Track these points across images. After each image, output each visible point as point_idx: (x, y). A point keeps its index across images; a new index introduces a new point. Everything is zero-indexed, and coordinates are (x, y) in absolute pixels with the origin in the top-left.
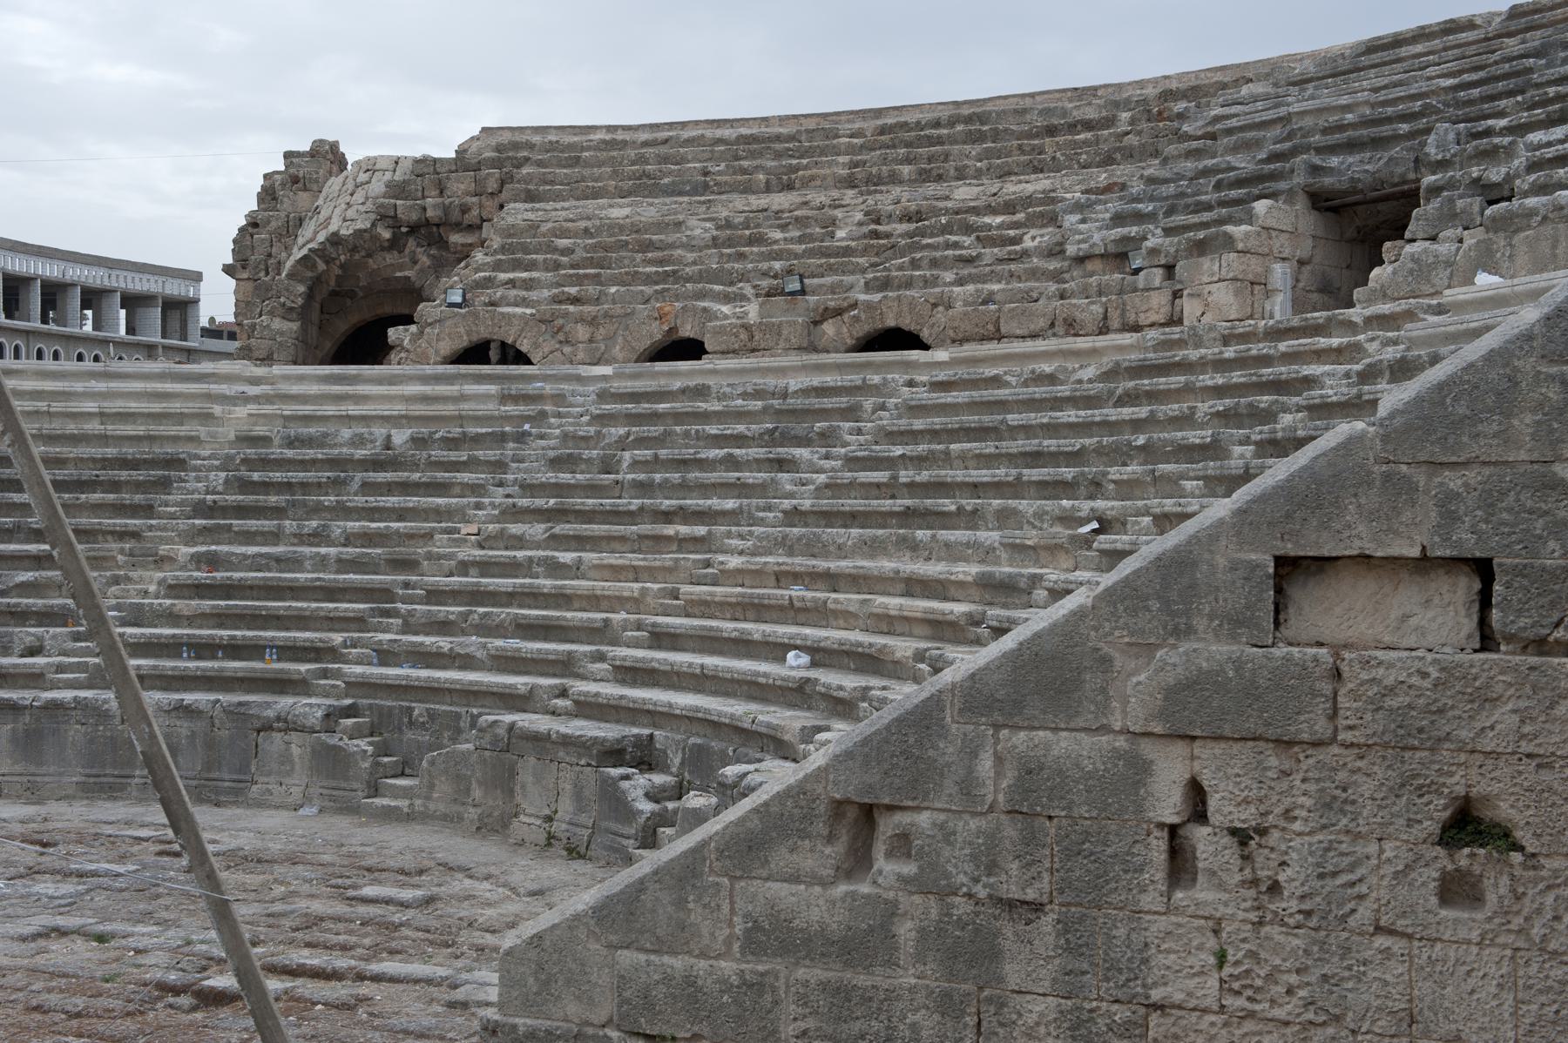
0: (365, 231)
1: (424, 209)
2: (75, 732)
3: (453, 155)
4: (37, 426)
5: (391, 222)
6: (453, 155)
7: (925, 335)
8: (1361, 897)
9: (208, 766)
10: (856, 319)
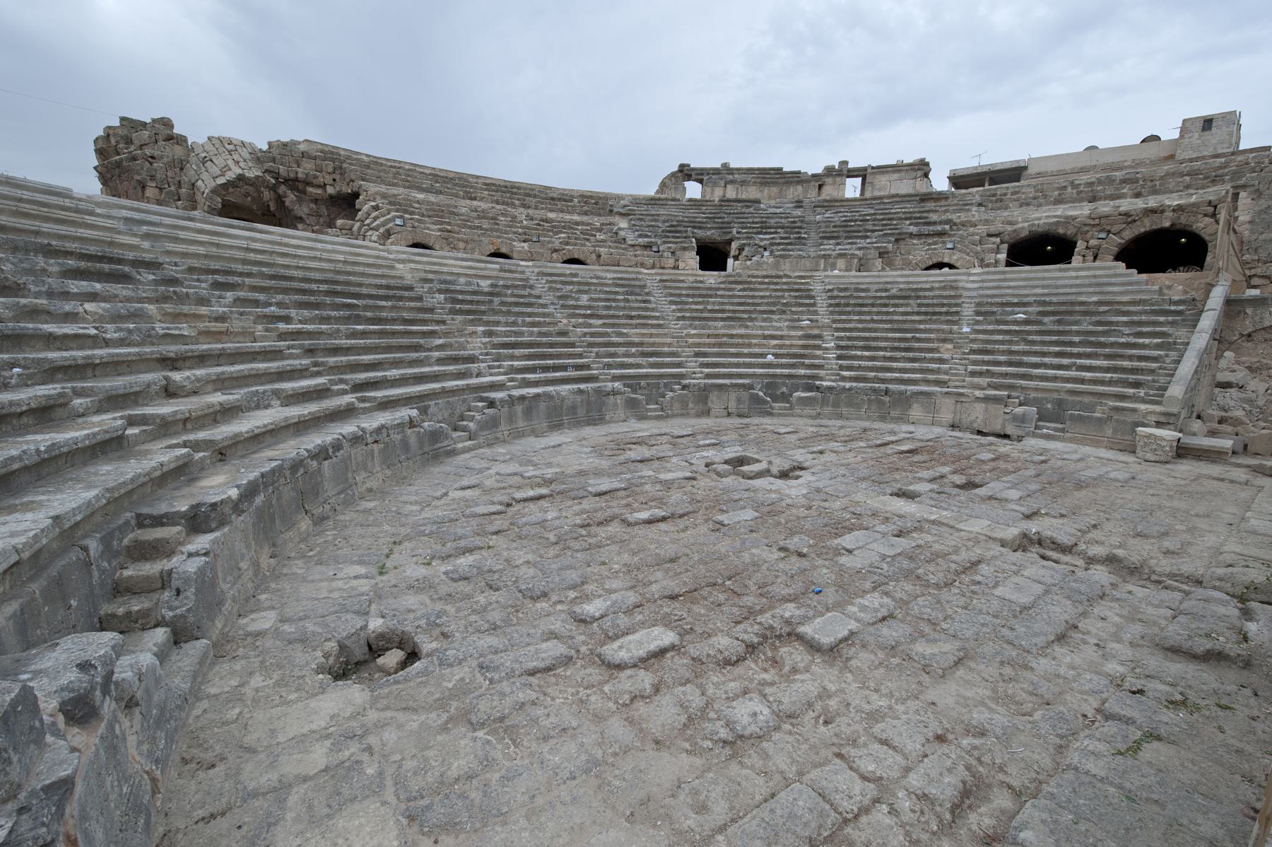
2: (543, 406)
3: (265, 147)
6: (265, 147)
7: (588, 261)
9: (587, 412)
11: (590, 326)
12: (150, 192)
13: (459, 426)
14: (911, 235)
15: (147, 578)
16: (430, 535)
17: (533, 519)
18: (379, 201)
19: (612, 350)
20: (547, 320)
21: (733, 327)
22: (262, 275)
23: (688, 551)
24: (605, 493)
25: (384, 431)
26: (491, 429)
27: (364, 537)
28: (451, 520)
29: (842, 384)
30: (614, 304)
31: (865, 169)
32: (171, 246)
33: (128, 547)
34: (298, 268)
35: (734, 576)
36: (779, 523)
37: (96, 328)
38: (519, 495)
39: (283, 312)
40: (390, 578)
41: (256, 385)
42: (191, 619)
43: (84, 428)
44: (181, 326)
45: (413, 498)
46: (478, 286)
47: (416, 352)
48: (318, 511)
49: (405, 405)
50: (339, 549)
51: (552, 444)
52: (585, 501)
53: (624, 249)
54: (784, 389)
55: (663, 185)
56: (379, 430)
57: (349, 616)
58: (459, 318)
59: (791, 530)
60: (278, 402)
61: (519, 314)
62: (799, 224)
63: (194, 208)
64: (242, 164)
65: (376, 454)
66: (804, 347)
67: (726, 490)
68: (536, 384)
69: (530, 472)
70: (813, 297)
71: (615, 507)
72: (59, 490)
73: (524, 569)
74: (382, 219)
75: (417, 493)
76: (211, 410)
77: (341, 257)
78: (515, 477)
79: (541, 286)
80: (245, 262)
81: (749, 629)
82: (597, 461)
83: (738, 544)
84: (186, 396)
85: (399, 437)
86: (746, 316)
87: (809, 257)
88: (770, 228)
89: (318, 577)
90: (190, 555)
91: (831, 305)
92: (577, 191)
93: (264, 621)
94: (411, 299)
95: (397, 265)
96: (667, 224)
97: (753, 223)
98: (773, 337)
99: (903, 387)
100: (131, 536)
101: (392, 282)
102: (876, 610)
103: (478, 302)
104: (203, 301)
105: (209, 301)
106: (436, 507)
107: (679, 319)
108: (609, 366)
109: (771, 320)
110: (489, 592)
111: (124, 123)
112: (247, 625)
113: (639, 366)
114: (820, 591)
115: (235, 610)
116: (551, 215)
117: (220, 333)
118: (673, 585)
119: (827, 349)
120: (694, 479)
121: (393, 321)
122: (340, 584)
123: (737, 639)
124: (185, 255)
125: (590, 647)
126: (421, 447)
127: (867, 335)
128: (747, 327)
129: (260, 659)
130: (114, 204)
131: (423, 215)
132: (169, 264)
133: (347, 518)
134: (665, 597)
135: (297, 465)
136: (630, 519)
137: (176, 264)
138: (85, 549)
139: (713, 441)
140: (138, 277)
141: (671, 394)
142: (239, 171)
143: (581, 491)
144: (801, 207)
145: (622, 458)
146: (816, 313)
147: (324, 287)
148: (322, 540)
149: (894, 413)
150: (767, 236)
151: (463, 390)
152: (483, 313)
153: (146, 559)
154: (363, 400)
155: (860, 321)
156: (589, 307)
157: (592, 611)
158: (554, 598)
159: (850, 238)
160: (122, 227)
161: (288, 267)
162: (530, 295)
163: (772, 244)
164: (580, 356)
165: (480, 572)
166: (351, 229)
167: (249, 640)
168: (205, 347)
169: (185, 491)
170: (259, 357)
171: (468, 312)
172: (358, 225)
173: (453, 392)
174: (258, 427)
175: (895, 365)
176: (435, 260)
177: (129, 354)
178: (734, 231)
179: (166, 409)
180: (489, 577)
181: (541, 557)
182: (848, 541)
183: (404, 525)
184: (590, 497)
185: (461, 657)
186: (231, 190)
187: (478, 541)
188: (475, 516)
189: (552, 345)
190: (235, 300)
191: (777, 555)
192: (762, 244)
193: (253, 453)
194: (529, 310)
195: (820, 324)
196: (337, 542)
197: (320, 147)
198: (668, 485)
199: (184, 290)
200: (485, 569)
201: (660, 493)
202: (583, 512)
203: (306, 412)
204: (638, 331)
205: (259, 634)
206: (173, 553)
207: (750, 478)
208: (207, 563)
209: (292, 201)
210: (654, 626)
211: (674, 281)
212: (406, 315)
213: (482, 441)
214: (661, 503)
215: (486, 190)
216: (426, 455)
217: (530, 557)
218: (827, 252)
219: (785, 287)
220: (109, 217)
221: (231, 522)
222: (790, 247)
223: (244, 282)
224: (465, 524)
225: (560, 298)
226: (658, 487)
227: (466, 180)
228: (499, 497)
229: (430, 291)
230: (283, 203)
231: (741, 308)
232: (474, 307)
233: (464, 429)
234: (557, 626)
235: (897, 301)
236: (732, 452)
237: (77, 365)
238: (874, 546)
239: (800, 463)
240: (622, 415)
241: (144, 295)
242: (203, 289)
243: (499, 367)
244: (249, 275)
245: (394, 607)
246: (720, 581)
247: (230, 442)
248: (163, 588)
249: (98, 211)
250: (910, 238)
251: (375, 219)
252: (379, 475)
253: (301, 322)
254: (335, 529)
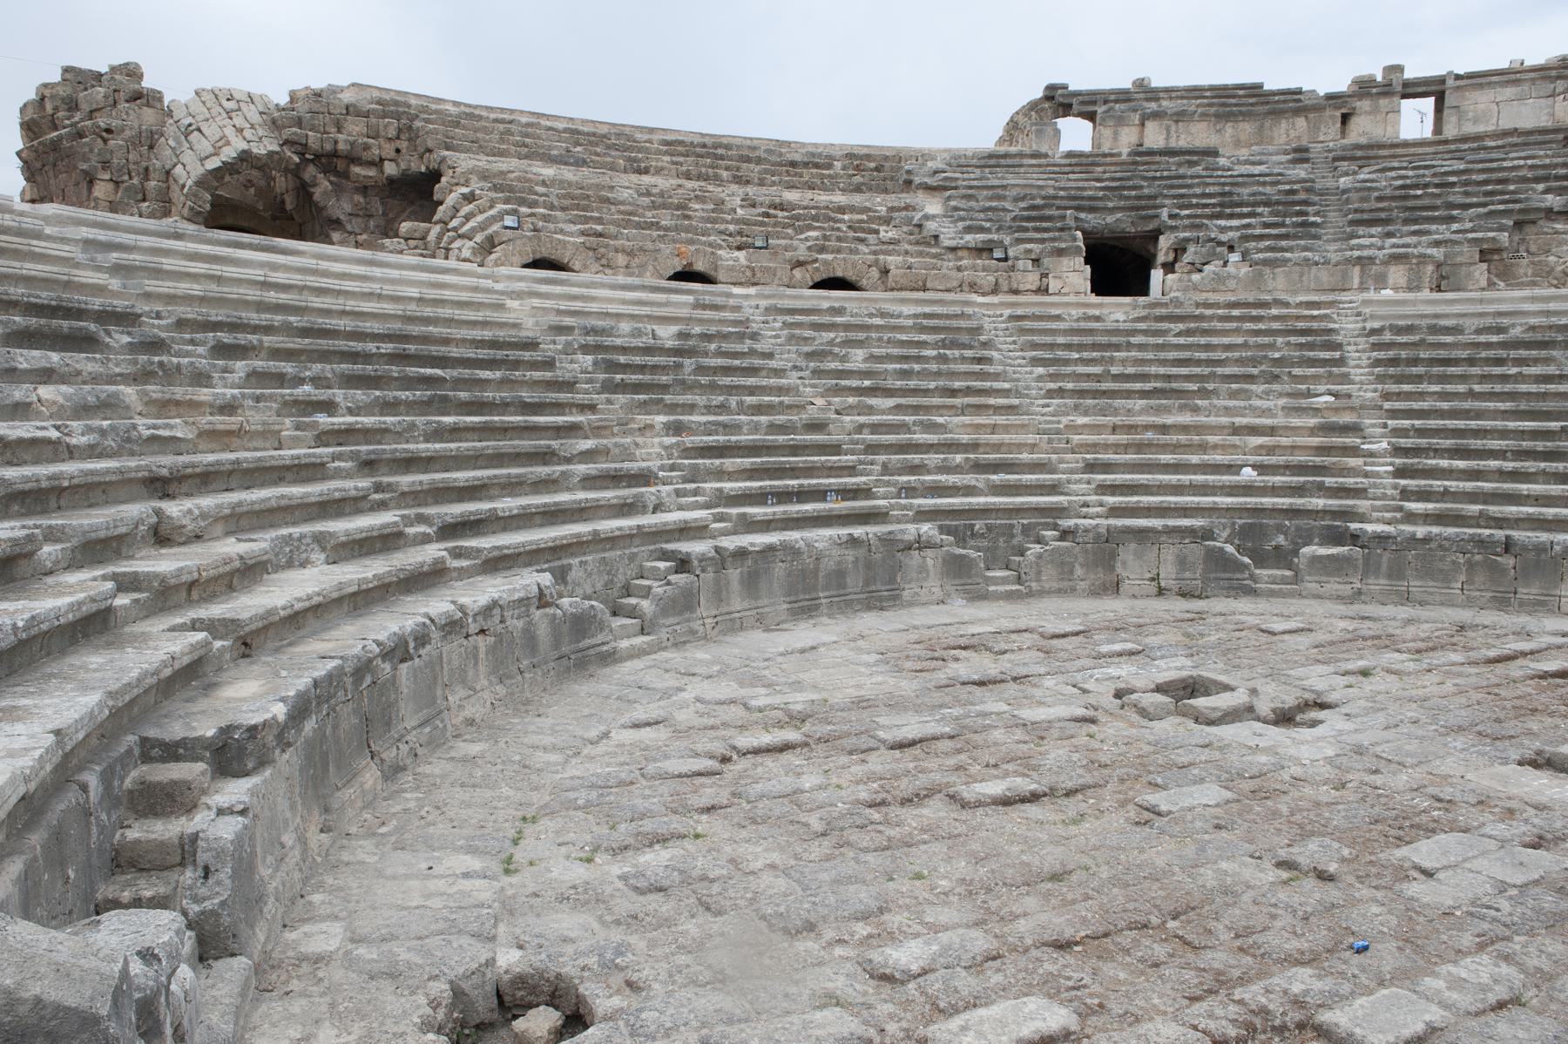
0: (277, 153)
1: (336, 142)
2: (779, 569)
4: (402, 307)
5: (299, 148)
6: (284, 100)
7: (864, 282)
9: (867, 583)
10: (817, 269)
11: (870, 410)
12: (101, 190)
13: (622, 607)
14: (1550, 213)
15: (162, 846)
16: (586, 807)
17: (775, 786)
18: (476, 185)
19: (915, 458)
20: (786, 400)
21: (1167, 410)
22: (288, 329)
23: (1086, 860)
24: (912, 743)
25: (497, 611)
26: (681, 613)
27: (469, 806)
28: (622, 784)
29: (1408, 528)
30: (917, 367)
31: (1441, 80)
32: (152, 285)
33: (131, 792)
34: (344, 313)
35: (1185, 913)
36: (1276, 814)
37: (57, 428)
38: (745, 741)
39: (322, 394)
40: (522, 882)
41: (287, 524)
42: (226, 920)
43: (61, 594)
44: (172, 422)
45: (548, 740)
46: (654, 337)
47: (545, 464)
48: (389, 755)
49: (527, 565)
50: (429, 824)
51: (799, 645)
52: (872, 757)
53: (936, 256)
54: (1281, 539)
55: (1013, 127)
56: (488, 610)
57: (465, 941)
58: (622, 399)
59: (1301, 826)
60: (323, 556)
61: (731, 390)
62: (1302, 196)
63: (167, 213)
64: (248, 133)
65: (482, 656)
66: (1322, 450)
67: (1160, 746)
68: (766, 525)
69: (761, 698)
70: (1339, 346)
71: (935, 769)
72: (42, 692)
73: (767, 878)
74: (480, 218)
75: (554, 732)
76: (228, 568)
77: (413, 292)
78: (733, 708)
79: (772, 335)
80: (261, 306)
81: (1219, 1012)
82: (891, 681)
83: (1190, 850)
84: (184, 543)
85: (520, 624)
86: (1193, 387)
87: (1327, 262)
88: (1240, 205)
89: (401, 870)
90: (221, 812)
91: (1377, 363)
92: (841, 146)
93: (324, 938)
94: (534, 365)
95: (510, 303)
96: (1023, 205)
97: (1204, 195)
98: (1253, 430)
99: (1544, 537)
100: (134, 774)
101: (501, 334)
102: (1484, 989)
103: (655, 368)
104: (201, 378)
105: (210, 377)
106: (591, 758)
107: (1050, 394)
108: (910, 491)
109: (1248, 395)
110: (703, 917)
111: (68, 76)
112: (297, 942)
113: (969, 491)
114: (1366, 948)
115: (279, 916)
116: (791, 196)
117: (230, 433)
118: (1061, 924)
119: (1371, 454)
120: (1093, 721)
121: (504, 407)
122: (441, 884)
123: (1195, 1028)
124: (171, 299)
125: (904, 1024)
126: (557, 644)
127: (1460, 424)
128: (1196, 410)
129: (328, 999)
130: (69, 218)
131: (552, 207)
132: (148, 315)
133: (437, 771)
134: (1045, 944)
135: (363, 668)
136: (965, 794)
137: (158, 316)
138: (84, 788)
139: (1129, 646)
140: (108, 340)
141: (1037, 548)
142: (243, 146)
143: (864, 738)
144: (1306, 160)
145: (941, 676)
146: (1345, 379)
147: (387, 348)
148: (398, 808)
149: (1528, 592)
150: (1235, 223)
151: (631, 536)
152: (664, 388)
153: (156, 815)
154: (457, 553)
155: (1444, 396)
156: (867, 374)
157: (904, 960)
158: (829, 934)
159: (1416, 221)
160: (77, 254)
161: (327, 313)
162: (752, 352)
163: (1246, 238)
164: (851, 470)
165: (687, 879)
166: (423, 238)
167: (306, 968)
168: (211, 458)
169: (202, 704)
170: (289, 476)
171: (637, 388)
172: (436, 229)
173: (612, 541)
174: (299, 600)
175: (1524, 488)
176: (575, 290)
177: (108, 471)
178: (1165, 213)
179: (164, 563)
180: (703, 889)
181: (797, 857)
182: (1424, 852)
183: (536, 789)
184: (883, 750)
185: (668, 1025)
186: (227, 178)
187: (676, 824)
188: (665, 777)
189: (795, 450)
190: (249, 375)
191: (1273, 874)
192: (1224, 238)
193: (290, 645)
194: (751, 381)
195: (1355, 402)
196: (423, 813)
197: (376, 94)
198: (1039, 732)
199: (175, 360)
200: (695, 873)
201: (1025, 747)
202: (870, 778)
203: (370, 575)
204: (966, 419)
205: (318, 960)
206: (195, 806)
207: (1211, 723)
208: (246, 827)
209: (325, 193)
210: (1026, 995)
211: (1040, 318)
212: (526, 395)
213: (665, 637)
214: (1028, 767)
215: (666, 153)
216: (565, 661)
217: (776, 857)
218: (1366, 253)
219: (1276, 325)
220: (63, 240)
221: (274, 761)
222: (1283, 243)
223: (261, 341)
224: (647, 792)
225: (810, 356)
226: (1019, 734)
227: (630, 138)
228: (705, 744)
229: (568, 350)
230: (310, 195)
231: (1184, 371)
232: (647, 378)
233: (632, 613)
234: (839, 984)
235: (1523, 353)
236: (1174, 668)
237: (40, 490)
238: (1481, 864)
239: (1319, 693)
240: (937, 590)
241: (117, 370)
242: (200, 356)
243: (696, 493)
244: (268, 329)
245: (537, 930)
246: (1155, 920)
247: (260, 624)
248: (182, 864)
249: (48, 230)
250: (1549, 219)
251: (468, 218)
252: (486, 695)
253: (351, 412)
254: (418, 788)
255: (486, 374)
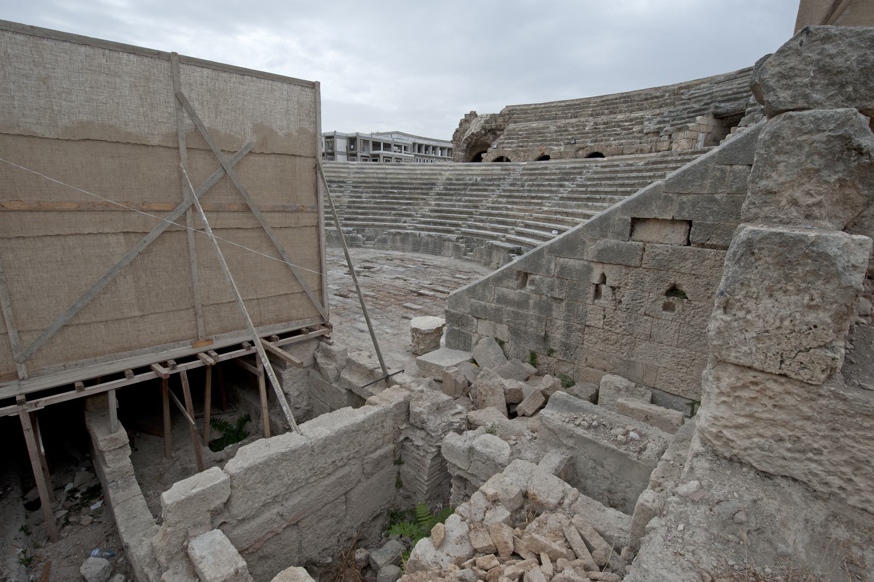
2: (411, 239)
7: (604, 154)
8: (642, 306)
255: (406, 191)
